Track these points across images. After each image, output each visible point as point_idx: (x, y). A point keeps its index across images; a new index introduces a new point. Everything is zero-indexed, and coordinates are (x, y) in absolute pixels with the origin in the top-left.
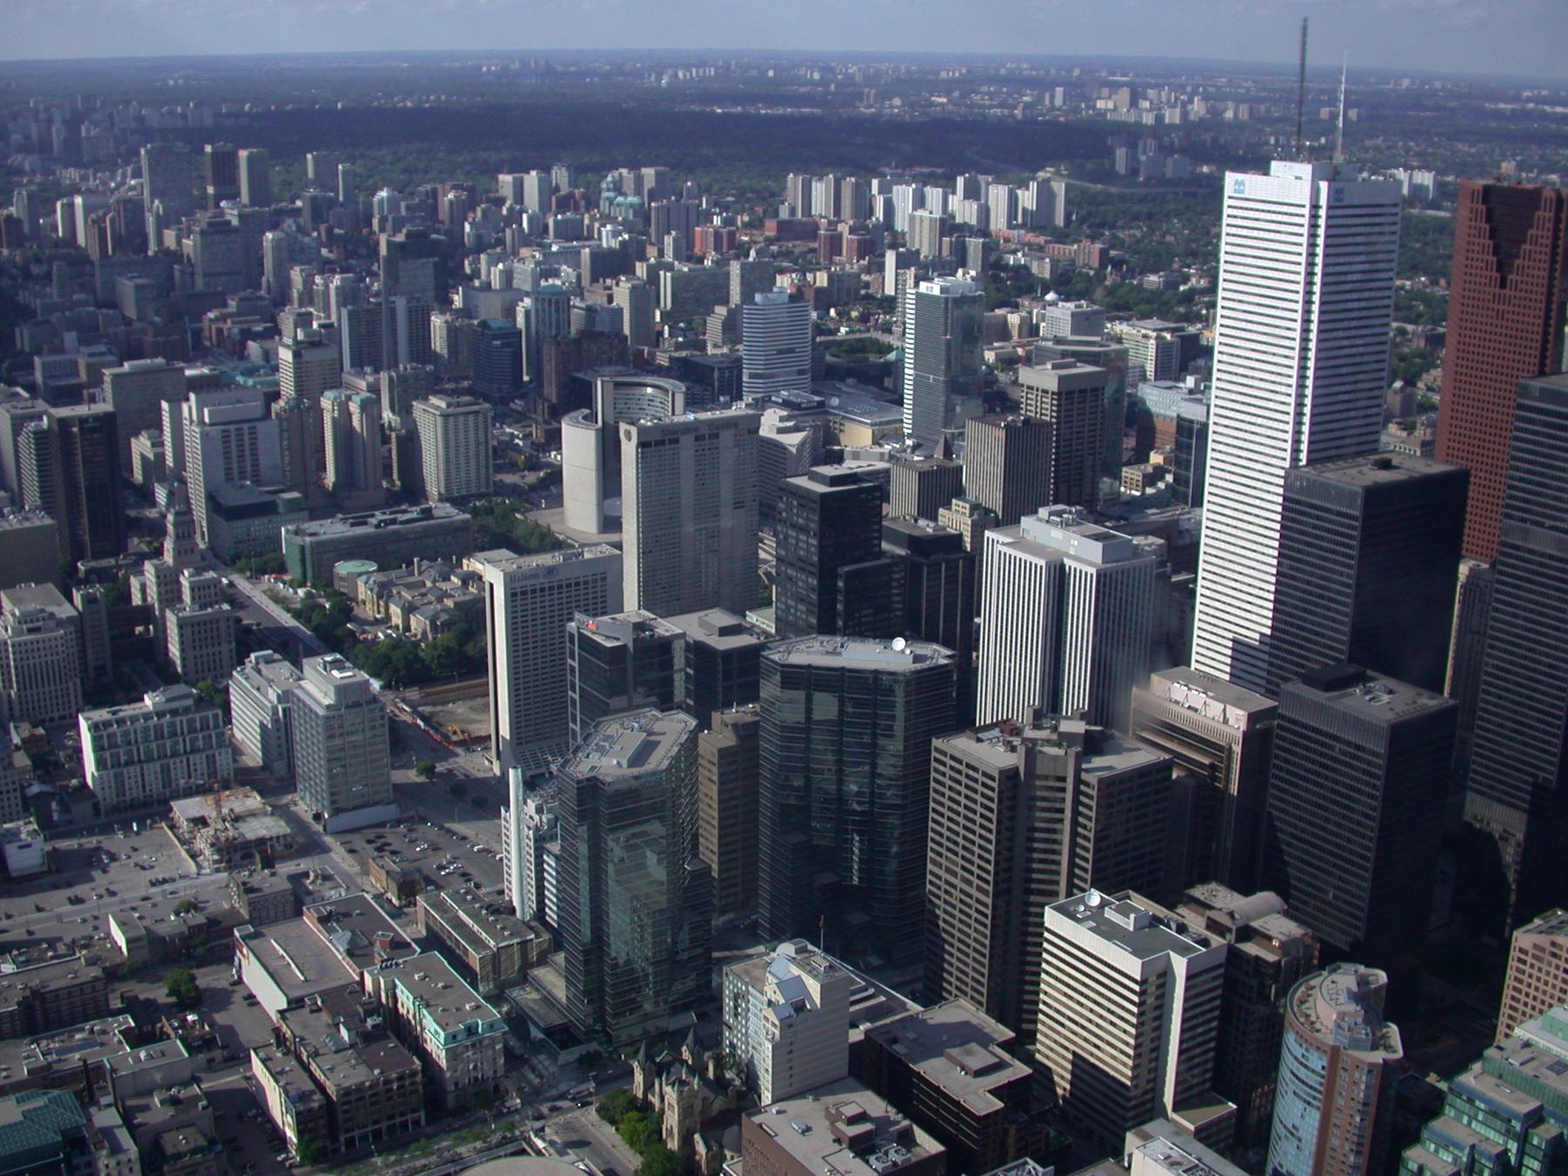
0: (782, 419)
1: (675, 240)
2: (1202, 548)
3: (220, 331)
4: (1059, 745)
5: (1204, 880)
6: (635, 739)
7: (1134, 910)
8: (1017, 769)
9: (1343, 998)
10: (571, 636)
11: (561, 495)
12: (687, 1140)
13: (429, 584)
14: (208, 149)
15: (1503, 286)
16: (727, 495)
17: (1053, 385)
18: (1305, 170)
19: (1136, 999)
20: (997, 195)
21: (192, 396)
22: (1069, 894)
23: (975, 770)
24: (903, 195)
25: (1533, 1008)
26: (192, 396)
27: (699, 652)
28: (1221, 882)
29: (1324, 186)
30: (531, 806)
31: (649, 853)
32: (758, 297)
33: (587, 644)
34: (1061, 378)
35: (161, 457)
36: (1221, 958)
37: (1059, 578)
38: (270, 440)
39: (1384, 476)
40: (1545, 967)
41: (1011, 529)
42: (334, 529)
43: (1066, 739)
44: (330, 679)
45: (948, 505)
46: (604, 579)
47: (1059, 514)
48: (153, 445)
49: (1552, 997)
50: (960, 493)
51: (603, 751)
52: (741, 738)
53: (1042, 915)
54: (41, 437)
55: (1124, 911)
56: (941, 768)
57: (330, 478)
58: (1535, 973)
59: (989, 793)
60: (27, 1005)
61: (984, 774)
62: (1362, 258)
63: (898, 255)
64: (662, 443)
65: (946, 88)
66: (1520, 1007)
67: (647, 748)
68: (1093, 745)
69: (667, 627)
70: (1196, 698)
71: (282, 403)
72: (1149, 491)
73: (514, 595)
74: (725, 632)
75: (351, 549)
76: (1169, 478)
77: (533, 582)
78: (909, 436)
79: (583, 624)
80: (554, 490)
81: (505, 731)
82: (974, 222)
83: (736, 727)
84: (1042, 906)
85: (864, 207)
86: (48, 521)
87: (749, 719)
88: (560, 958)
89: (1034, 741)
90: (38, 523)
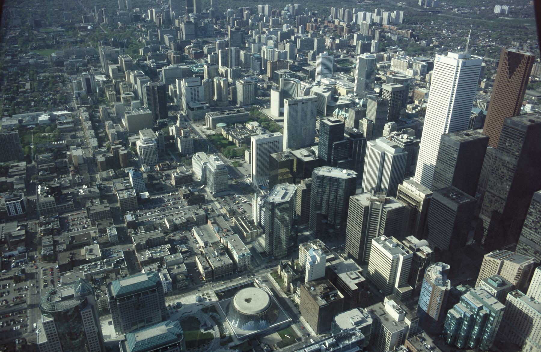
0: (324, 89)
3: (189, 51)
4: (379, 202)
8: (368, 206)
9: (438, 273)
11: (270, 105)
12: (289, 284)
16: (309, 116)
17: (390, 90)
20: (385, 15)
24: (361, 14)
27: (299, 160)
32: (320, 54)
34: (393, 88)
35: (176, 91)
36: (412, 256)
37: (384, 155)
38: (201, 89)
41: (373, 141)
50: (365, 116)
54: (148, 88)
57: (215, 98)
60: (147, 242)
63: (358, 35)
67: (286, 194)
68: (387, 202)
70: (413, 189)
71: (204, 80)
72: (414, 112)
74: (306, 156)
78: (356, 92)
81: (254, 173)
82: (378, 22)
85: (350, 19)
86: (150, 112)
87: (310, 182)
88: (264, 236)
90: (147, 112)
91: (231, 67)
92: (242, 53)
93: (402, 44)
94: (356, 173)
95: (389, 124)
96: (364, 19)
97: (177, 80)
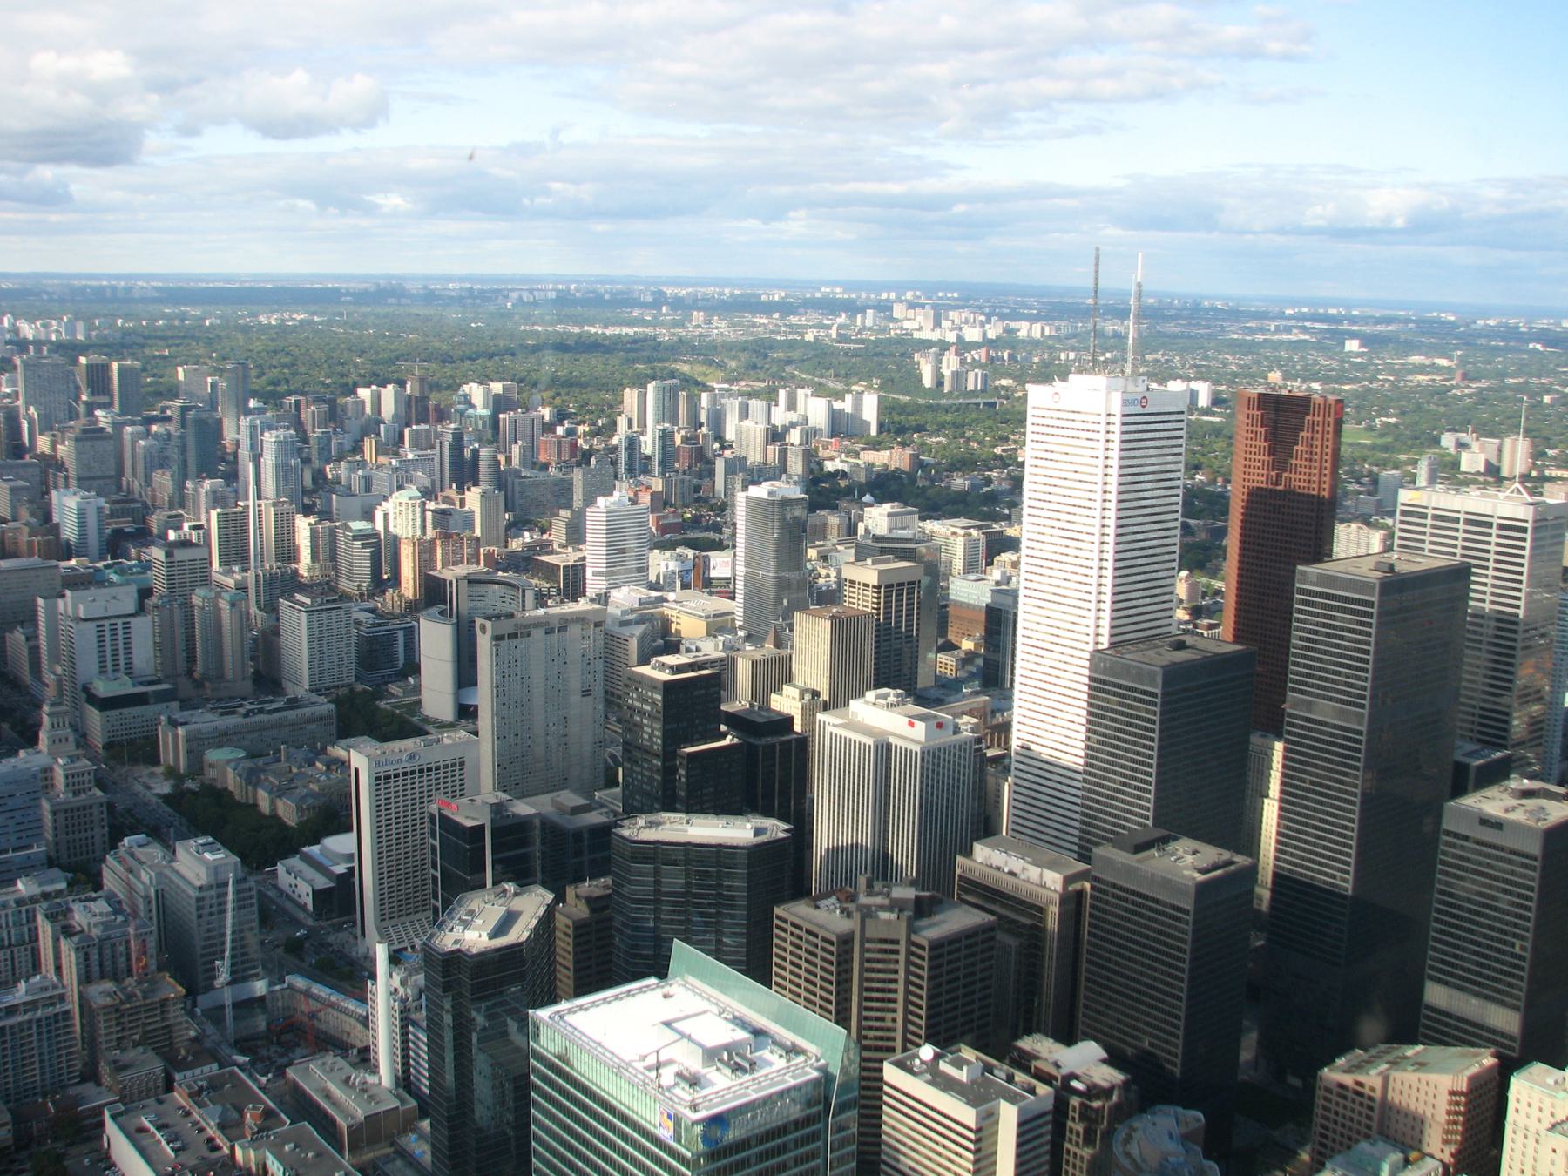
1: (523, 448)
4: (890, 909)
5: (1029, 1032)
6: (495, 912)
7: (968, 1063)
10: (432, 817)
13: (295, 770)
14: (83, 360)
16: (575, 683)
17: (873, 579)
18: (1099, 381)
19: (971, 1146)
21: (68, 593)
22: (905, 1050)
23: (816, 936)
25: (1341, 1144)
26: (68, 593)
28: (1046, 1034)
29: (1117, 398)
30: (397, 979)
31: (509, 1021)
32: (601, 501)
33: (448, 825)
34: (880, 572)
39: (1180, 656)
40: (1349, 1104)
41: (841, 711)
42: (207, 720)
43: (897, 905)
44: (205, 862)
45: (779, 690)
46: (462, 764)
47: (885, 697)
48: (28, 639)
49: (1358, 1132)
51: (467, 925)
52: (593, 910)
53: (881, 1070)
55: (959, 1063)
56: (783, 934)
58: (1341, 1110)
59: (828, 956)
61: (824, 939)
62: (1154, 460)
63: (726, 461)
64: (515, 636)
65: (767, 309)
66: (1329, 1143)
67: (508, 920)
68: (923, 909)
69: (523, 808)
70: (1015, 864)
73: (378, 779)
75: (222, 739)
76: (980, 662)
78: (741, 628)
80: (411, 680)
83: (590, 900)
84: (881, 1061)
87: (598, 892)
88: (426, 1124)
89: (868, 907)
92: (303, 527)
93: (884, 486)
96: (745, 413)
97: (40, 601)
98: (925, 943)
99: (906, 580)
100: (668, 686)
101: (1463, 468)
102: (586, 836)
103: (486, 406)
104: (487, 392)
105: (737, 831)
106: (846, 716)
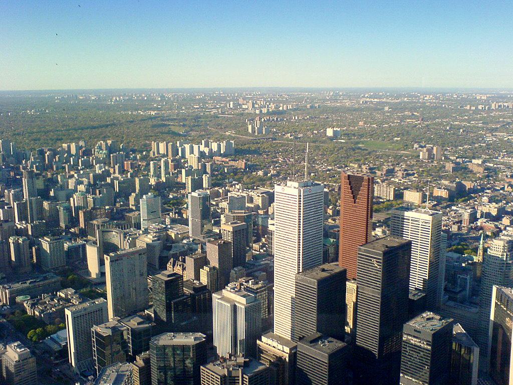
2: (275, 272)
15: (355, 203)
32: (144, 197)
33: (97, 334)
37: (235, 309)
63: (186, 170)
64: (118, 260)
70: (275, 344)
75: (21, 292)
77: (80, 313)
79: (96, 328)
85: (175, 152)
87: (148, 356)
91: (32, 222)
94: (205, 336)
95: (236, 269)
96: (192, 152)
98: (247, 377)
99: (241, 229)
100: (167, 282)
101: (421, 157)
102: (142, 332)
103: (106, 150)
104: (107, 144)
105: (188, 339)
106: (221, 295)
